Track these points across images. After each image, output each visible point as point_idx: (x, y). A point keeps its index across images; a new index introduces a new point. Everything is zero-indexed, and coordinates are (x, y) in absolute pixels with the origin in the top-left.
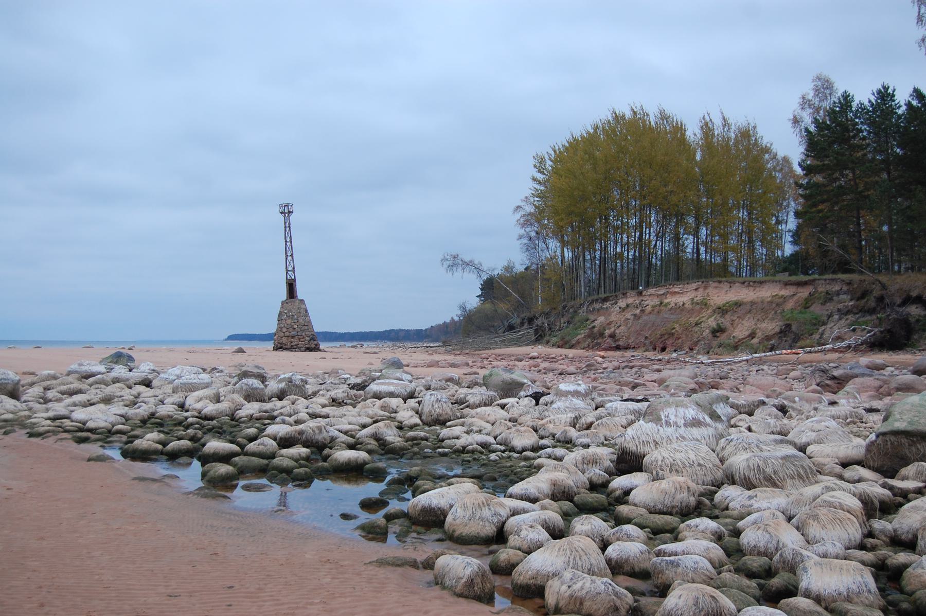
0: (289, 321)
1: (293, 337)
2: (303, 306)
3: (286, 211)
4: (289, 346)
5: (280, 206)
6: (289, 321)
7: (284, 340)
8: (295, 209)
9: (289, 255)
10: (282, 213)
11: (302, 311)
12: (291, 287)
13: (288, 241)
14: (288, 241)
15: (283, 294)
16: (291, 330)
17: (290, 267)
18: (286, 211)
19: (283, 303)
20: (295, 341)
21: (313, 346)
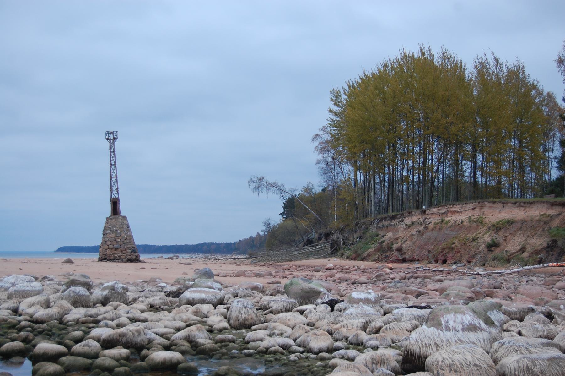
0: (113, 235)
1: (116, 249)
2: (125, 222)
3: (112, 138)
4: (112, 258)
5: (106, 133)
6: (113, 235)
7: (108, 252)
8: (119, 136)
9: (114, 177)
10: (107, 139)
11: (124, 226)
12: (115, 204)
13: (113, 164)
14: (113, 164)
16: (114, 243)
17: (114, 187)
18: (112, 138)
19: (108, 219)
20: (118, 253)
21: (134, 257)
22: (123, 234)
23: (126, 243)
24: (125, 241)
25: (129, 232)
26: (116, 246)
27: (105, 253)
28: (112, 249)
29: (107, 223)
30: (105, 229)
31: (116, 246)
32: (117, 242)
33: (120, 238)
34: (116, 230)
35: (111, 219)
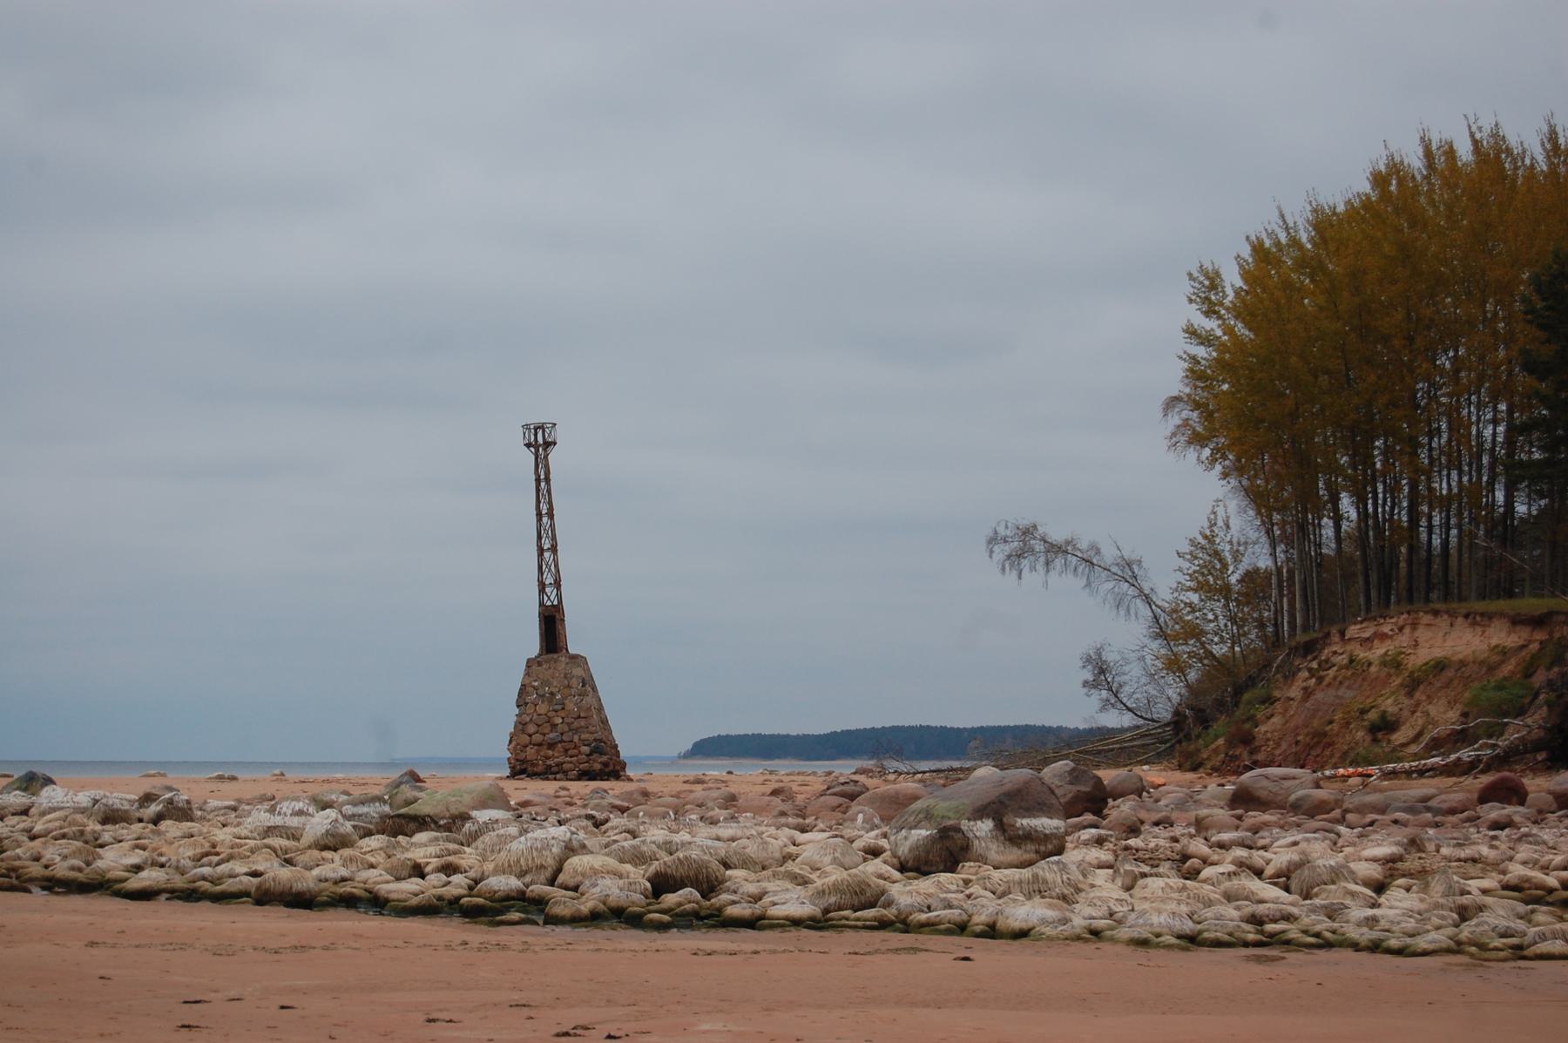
0: (543, 708)
1: (551, 746)
2: (578, 672)
3: (540, 442)
5: (526, 427)
6: (543, 708)
7: (530, 752)
8: (560, 435)
9: (547, 547)
10: (528, 445)
11: (574, 682)
12: (551, 623)
13: (545, 512)
14: (545, 512)
15: (533, 646)
18: (540, 442)
19: (530, 663)
22: (570, 705)
23: (576, 730)
24: (576, 724)
25: (589, 700)
26: (552, 735)
27: (522, 756)
28: (540, 745)
29: (527, 674)
30: (523, 691)
31: (552, 735)
32: (554, 726)
33: (562, 714)
34: (552, 694)
35: (540, 664)
